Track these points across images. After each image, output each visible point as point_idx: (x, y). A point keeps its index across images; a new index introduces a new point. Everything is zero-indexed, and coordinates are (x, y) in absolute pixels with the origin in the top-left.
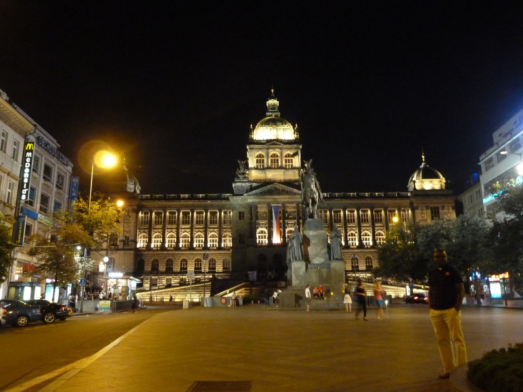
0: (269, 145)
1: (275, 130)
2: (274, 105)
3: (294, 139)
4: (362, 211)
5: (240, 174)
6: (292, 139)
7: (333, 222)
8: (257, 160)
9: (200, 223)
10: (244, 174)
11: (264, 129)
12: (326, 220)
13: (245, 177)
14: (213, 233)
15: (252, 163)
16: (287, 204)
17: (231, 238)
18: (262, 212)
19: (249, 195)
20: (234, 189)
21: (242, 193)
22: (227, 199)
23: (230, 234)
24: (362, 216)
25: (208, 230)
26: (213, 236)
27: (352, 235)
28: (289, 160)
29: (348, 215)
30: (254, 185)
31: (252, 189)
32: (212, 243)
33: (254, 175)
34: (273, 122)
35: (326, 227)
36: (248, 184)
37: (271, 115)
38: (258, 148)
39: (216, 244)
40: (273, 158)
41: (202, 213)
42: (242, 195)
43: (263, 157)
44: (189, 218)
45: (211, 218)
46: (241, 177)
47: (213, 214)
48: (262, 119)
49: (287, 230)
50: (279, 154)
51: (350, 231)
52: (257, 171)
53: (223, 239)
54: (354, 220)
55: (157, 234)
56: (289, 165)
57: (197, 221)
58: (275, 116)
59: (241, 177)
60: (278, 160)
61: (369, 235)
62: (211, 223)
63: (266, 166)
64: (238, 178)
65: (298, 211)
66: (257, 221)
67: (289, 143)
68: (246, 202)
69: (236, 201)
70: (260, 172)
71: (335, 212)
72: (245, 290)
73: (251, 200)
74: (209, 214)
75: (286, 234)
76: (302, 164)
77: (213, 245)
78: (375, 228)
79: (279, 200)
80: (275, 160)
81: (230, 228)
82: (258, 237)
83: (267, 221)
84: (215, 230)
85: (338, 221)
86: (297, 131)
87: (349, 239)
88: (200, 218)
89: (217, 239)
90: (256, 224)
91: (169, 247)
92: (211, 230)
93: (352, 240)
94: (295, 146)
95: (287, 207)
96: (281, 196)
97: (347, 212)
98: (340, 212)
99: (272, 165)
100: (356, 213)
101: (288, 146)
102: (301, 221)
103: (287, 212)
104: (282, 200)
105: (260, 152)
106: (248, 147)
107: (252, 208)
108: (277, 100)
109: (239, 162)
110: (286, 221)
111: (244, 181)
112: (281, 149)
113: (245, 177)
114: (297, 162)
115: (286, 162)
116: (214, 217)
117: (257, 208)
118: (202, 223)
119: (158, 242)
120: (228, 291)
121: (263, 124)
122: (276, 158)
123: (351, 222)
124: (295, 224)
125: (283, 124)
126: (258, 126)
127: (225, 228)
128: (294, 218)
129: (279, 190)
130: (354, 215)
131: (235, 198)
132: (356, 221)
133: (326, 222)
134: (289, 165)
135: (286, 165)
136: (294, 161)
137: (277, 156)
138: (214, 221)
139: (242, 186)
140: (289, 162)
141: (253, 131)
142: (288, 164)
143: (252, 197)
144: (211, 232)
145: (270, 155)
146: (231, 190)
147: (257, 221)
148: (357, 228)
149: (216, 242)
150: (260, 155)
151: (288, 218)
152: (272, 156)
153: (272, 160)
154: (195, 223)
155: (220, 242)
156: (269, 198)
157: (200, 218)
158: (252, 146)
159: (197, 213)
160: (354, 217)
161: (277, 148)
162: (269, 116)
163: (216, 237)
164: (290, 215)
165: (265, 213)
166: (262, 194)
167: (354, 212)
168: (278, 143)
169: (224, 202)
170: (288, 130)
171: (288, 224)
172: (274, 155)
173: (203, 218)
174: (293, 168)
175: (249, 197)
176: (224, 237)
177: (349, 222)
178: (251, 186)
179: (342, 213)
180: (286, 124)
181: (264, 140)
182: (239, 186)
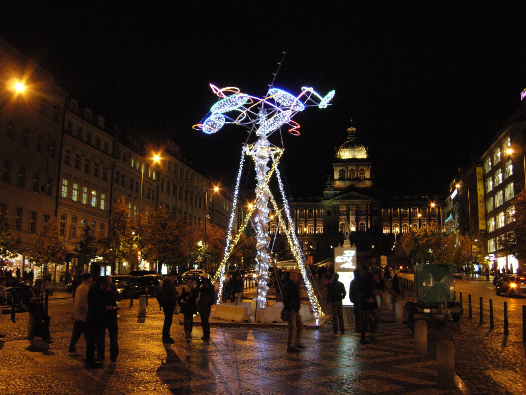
0: (348, 163)
1: (353, 151)
2: (352, 131)
3: (366, 158)
4: (412, 209)
5: (329, 185)
6: (364, 158)
7: (392, 217)
8: (340, 174)
9: (301, 218)
10: (331, 184)
11: (345, 151)
12: (388, 215)
13: (331, 187)
14: (310, 224)
15: (336, 176)
16: (360, 205)
17: (323, 228)
18: (343, 211)
19: (334, 200)
20: (324, 195)
21: (329, 198)
22: (319, 201)
23: (322, 225)
24: (413, 213)
25: (307, 222)
26: (310, 226)
27: (405, 225)
28: (362, 173)
29: (403, 212)
30: (338, 192)
31: (336, 195)
32: (310, 231)
33: (338, 184)
34: (351, 146)
35: (388, 220)
36: (333, 192)
37: (350, 139)
38: (340, 165)
39: (312, 232)
40: (351, 172)
41: (303, 210)
42: (329, 199)
43: (344, 171)
44: (294, 214)
45: (309, 214)
46: (329, 186)
47: (311, 211)
48: (344, 142)
49: (360, 223)
50: (355, 169)
51: (404, 222)
52: (340, 181)
53: (317, 228)
54: (407, 215)
55: (274, 224)
56: (362, 177)
57: (299, 216)
58: (353, 140)
59: (329, 186)
60: (354, 173)
61: (417, 226)
62: (309, 217)
63: (346, 178)
64: (327, 187)
65: (367, 210)
66: (339, 217)
67: (362, 160)
68: (332, 204)
69: (327, 203)
70: (342, 182)
71: (393, 210)
72: (330, 263)
73: (335, 203)
74: (307, 211)
75: (359, 226)
76: (371, 175)
77: (311, 232)
78: (421, 221)
79: (354, 203)
80: (352, 173)
81: (321, 221)
82: (340, 228)
83: (346, 217)
84: (312, 222)
85: (395, 216)
86: (368, 152)
87: (403, 228)
88: (301, 214)
89: (313, 228)
90: (338, 218)
91: (281, 233)
92: (309, 222)
93: (405, 229)
94: (367, 163)
95: (360, 207)
96: (356, 201)
97: (402, 209)
98: (397, 209)
99: (350, 177)
100: (408, 210)
101: (362, 163)
102: (369, 217)
103: (360, 211)
104: (356, 203)
105: (342, 168)
106: (334, 164)
107: (336, 208)
108: (355, 128)
109: (327, 175)
110: (359, 217)
111: (331, 189)
112: (357, 165)
113: (331, 187)
114: (367, 175)
115: (360, 175)
116: (311, 213)
117: (339, 208)
118: (303, 218)
119: (274, 230)
120: (320, 263)
121: (344, 148)
122: (353, 172)
123: (405, 216)
124: (364, 219)
125: (358, 147)
126: (341, 149)
127: (318, 221)
128: (364, 215)
129: (354, 196)
130: (407, 212)
131: (324, 201)
132: (408, 216)
133: (388, 217)
134: (362, 177)
135: (360, 177)
136: (365, 174)
137: (354, 170)
138: (311, 216)
139: (329, 193)
140: (362, 175)
141: (337, 152)
142: (361, 176)
143: (336, 201)
144: (309, 223)
145: (349, 169)
146: (322, 195)
147: (339, 217)
148: (408, 221)
149: (312, 230)
150: (342, 169)
151: (360, 215)
152: (350, 171)
153: (350, 173)
154: (298, 217)
155: (315, 231)
156: (347, 202)
157: (301, 214)
158: (336, 164)
159: (299, 210)
160: (407, 213)
161: (353, 165)
162: (349, 140)
163: (312, 227)
164: (362, 213)
165: (345, 211)
166: (343, 199)
167: (407, 209)
168: (355, 161)
169: (317, 203)
170: (362, 151)
171: (360, 219)
172: (352, 170)
173: (303, 214)
174: (365, 179)
175: (334, 201)
176: (318, 227)
177: (403, 216)
178: (336, 193)
179: (399, 210)
180: (360, 147)
181: (345, 159)
182: (327, 193)
